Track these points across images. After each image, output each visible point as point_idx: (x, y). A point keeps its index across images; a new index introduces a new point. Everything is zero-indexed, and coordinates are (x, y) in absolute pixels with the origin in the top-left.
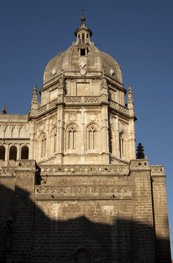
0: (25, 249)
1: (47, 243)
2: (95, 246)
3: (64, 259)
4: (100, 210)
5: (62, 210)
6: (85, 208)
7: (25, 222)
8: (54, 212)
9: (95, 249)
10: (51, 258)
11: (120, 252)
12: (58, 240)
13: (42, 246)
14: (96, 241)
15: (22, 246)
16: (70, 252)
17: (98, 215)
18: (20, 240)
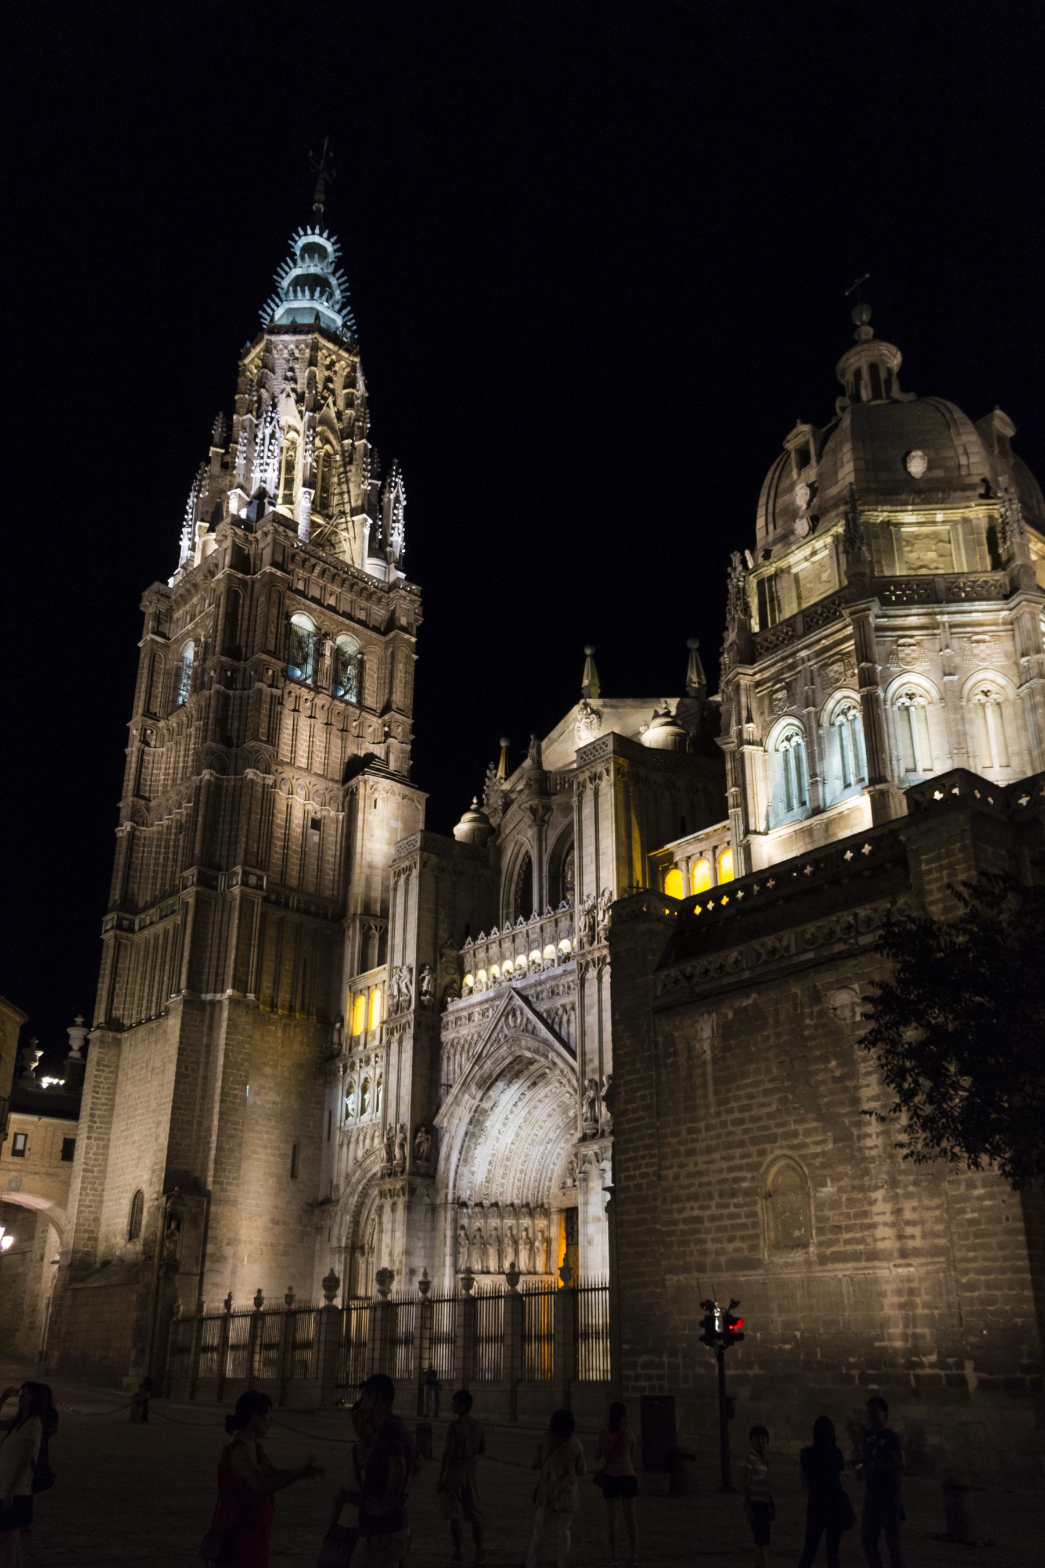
0: (644, 1181)
1: (691, 1153)
2: (816, 1143)
3: (736, 1201)
4: (819, 1008)
5: (720, 1032)
6: (778, 1014)
7: (638, 1094)
8: (702, 1048)
9: (815, 1156)
10: (706, 1203)
11: (892, 1156)
12: (719, 1136)
13: (682, 1166)
14: (815, 1124)
15: (637, 1173)
16: (749, 1175)
17: (816, 1027)
18: (631, 1154)
